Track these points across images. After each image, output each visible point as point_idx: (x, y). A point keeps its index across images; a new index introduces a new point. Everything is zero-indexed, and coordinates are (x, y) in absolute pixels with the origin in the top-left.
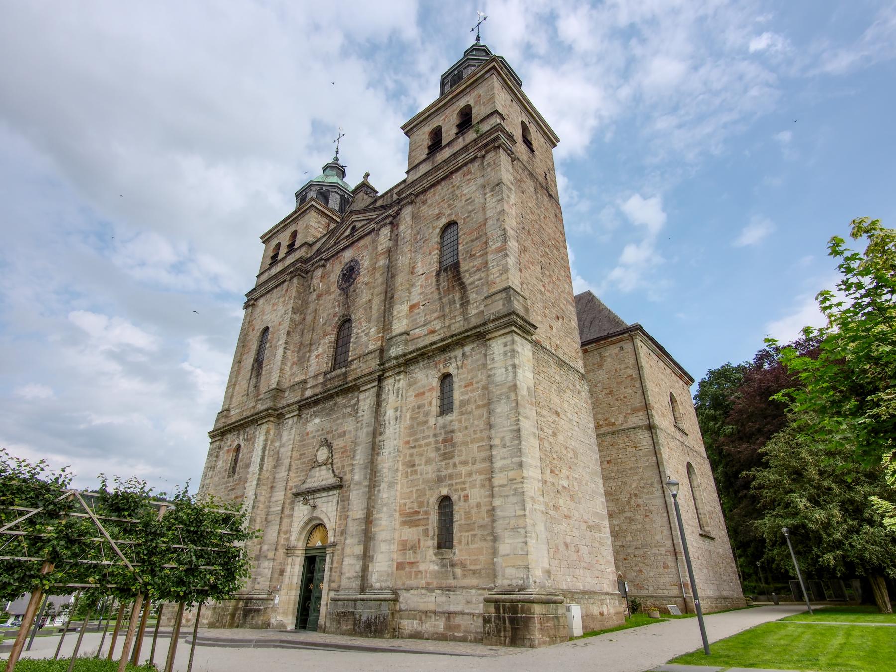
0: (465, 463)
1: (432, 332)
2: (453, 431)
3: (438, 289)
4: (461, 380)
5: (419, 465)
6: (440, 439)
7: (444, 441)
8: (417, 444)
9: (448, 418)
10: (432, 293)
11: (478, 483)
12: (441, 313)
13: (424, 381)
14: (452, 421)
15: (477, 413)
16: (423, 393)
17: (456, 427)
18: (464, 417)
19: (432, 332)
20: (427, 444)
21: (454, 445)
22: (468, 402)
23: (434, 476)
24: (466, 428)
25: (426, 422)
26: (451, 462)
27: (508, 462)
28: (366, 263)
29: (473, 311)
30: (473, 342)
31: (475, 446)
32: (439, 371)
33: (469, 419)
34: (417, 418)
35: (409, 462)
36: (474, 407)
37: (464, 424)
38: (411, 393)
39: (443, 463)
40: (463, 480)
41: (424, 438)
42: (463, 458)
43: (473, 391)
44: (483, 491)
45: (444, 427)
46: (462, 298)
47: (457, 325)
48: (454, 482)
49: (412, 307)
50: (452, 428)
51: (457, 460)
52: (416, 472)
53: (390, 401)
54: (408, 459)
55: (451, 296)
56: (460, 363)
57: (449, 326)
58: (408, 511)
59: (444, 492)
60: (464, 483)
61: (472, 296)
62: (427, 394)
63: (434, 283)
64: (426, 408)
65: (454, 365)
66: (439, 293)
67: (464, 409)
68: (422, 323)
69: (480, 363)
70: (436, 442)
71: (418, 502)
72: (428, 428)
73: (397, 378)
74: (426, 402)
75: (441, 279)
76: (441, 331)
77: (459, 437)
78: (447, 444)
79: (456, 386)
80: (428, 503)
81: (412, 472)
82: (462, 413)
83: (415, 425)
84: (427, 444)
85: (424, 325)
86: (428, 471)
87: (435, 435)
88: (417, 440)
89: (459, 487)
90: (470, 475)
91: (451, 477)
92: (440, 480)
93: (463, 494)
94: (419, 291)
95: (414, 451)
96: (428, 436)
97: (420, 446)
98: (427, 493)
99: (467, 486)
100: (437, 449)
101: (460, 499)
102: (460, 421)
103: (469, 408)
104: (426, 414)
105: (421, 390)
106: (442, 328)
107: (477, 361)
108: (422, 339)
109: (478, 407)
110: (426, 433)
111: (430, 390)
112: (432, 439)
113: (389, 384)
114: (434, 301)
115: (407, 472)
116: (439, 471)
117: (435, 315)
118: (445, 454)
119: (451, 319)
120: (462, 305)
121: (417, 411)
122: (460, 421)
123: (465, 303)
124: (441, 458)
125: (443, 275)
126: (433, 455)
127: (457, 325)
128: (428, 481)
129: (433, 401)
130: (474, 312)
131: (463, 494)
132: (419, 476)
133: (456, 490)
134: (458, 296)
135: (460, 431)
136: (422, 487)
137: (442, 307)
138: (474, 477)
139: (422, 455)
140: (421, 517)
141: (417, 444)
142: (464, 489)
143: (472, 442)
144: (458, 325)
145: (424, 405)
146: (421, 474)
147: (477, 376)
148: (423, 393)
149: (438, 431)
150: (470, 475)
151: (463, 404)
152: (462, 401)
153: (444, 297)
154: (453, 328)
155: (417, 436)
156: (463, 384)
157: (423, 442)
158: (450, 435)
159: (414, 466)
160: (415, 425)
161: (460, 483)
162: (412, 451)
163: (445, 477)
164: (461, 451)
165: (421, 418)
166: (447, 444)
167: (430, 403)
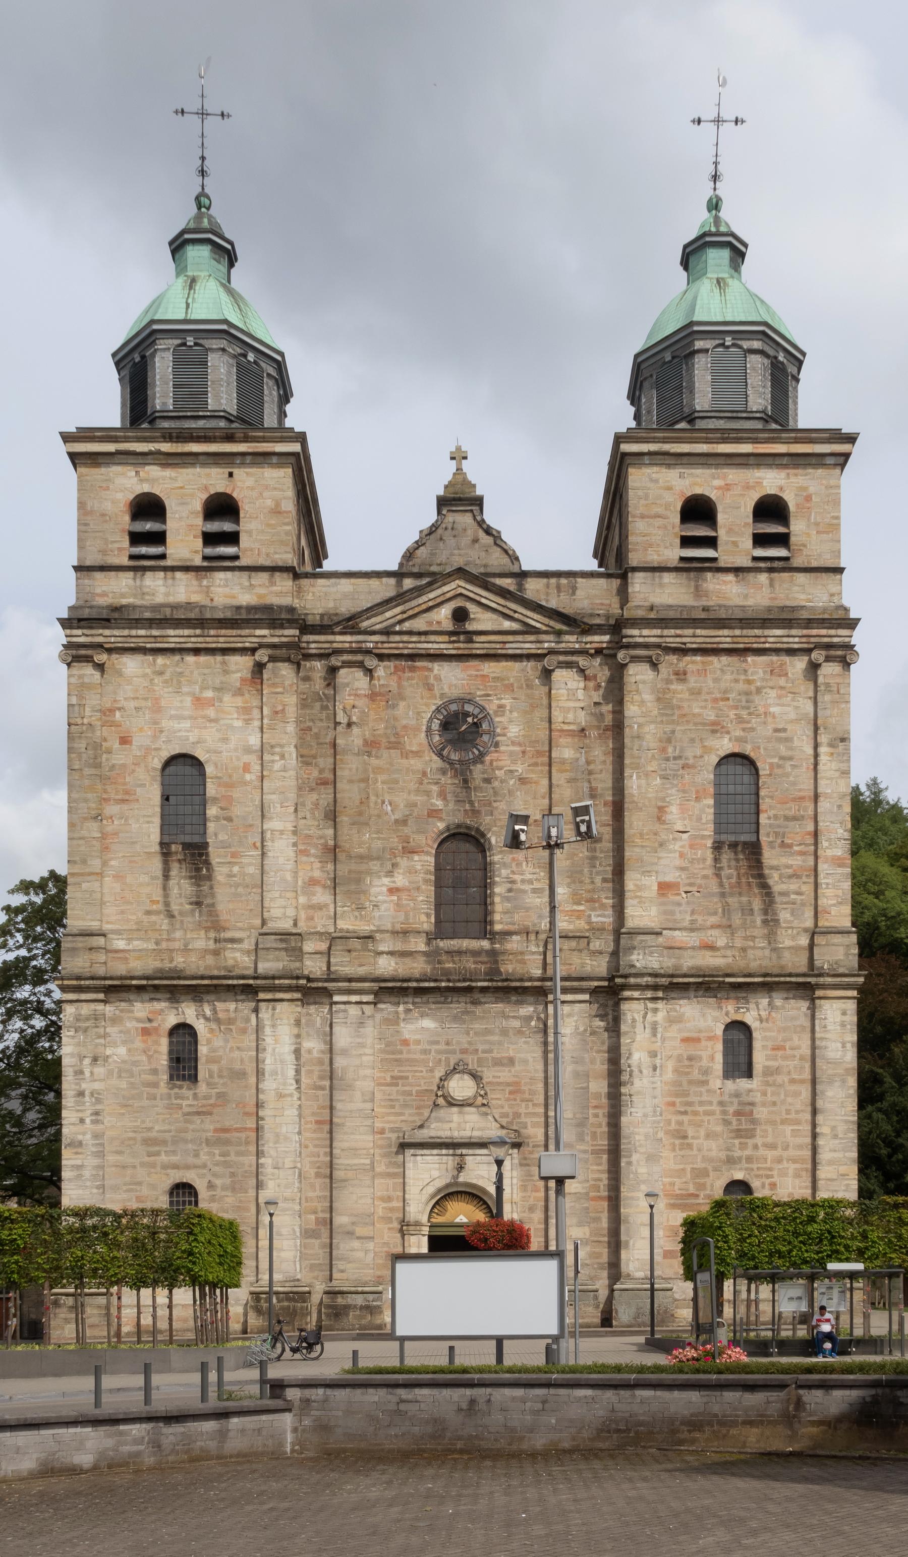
0: (772, 1147)
1: (711, 948)
2: (752, 1104)
3: (718, 876)
4: (765, 1038)
5: (693, 1138)
6: (731, 1110)
7: (738, 1113)
8: (689, 1109)
9: (743, 1084)
10: (705, 877)
11: (791, 1172)
12: (725, 922)
13: (702, 1024)
14: (750, 1091)
15: (793, 1088)
16: (698, 1040)
17: (758, 1098)
18: (770, 1090)
19: (711, 948)
20: (707, 1113)
21: (754, 1122)
22: (778, 1071)
23: (723, 1155)
24: (774, 1104)
25: (705, 1083)
26: (750, 1142)
27: (839, 1155)
28: (512, 726)
29: (786, 940)
30: (788, 990)
31: (788, 1129)
32: (727, 1014)
33: (779, 1094)
34: (688, 1073)
35: (678, 1131)
36: (786, 1080)
37: (769, 1098)
38: (674, 1032)
39: (737, 1141)
40: (768, 1165)
41: (701, 1103)
42: (770, 1140)
43: (785, 1058)
44: (797, 1181)
45: (737, 1095)
46: (765, 912)
47: (759, 953)
48: (755, 1166)
49: (664, 888)
50: (750, 1099)
51: (759, 1141)
52: (690, 1146)
53: (638, 1038)
54: (673, 1126)
55: (744, 899)
56: (764, 1014)
57: (744, 950)
58: (678, 1192)
59: (739, 1176)
60: (770, 1169)
61: (784, 915)
62: (704, 1043)
63: (709, 861)
64: (705, 1063)
65: (754, 1013)
66: (721, 885)
67: (770, 1079)
68: (686, 924)
69: (798, 1023)
70: (724, 1112)
71: (695, 1184)
72: (708, 1091)
73: (650, 1005)
74: (704, 1055)
75: (724, 863)
76: (729, 953)
77: (761, 1113)
78: (743, 1121)
79: (757, 1045)
80: (712, 1186)
81: (682, 1144)
82: (767, 1084)
83: (685, 1083)
84: (707, 1113)
85: (692, 930)
86: (714, 1149)
87: (721, 1103)
88: (690, 1104)
89: (761, 1172)
90: (779, 1160)
91: (749, 1159)
92: (731, 1161)
93: (768, 1181)
94: (678, 862)
95: (685, 1118)
96: (711, 1103)
97: (695, 1113)
98: (711, 1174)
99: (775, 1173)
100: (727, 1123)
101: (763, 1186)
102: (764, 1094)
103: (779, 1079)
104: (706, 1072)
105: (695, 1035)
106: (727, 947)
107: (793, 1018)
108: (690, 952)
109: (793, 1081)
110: (705, 1098)
111: (710, 1038)
112: (715, 1108)
113: (633, 1010)
114: (712, 895)
115: (674, 1144)
116: (728, 1149)
117: (713, 920)
118: (738, 1130)
119: (746, 938)
120: (765, 922)
121: (686, 1063)
122: (764, 1094)
123: (771, 922)
124: (732, 1135)
125: (727, 856)
126: (719, 1129)
127: (759, 953)
128: (711, 1160)
129: (714, 1055)
130: (788, 943)
131: (768, 1181)
132: (695, 1152)
133: (757, 1176)
134: (757, 904)
135: (764, 1104)
136: (700, 1165)
137: (727, 911)
138: (785, 1164)
139: (700, 1126)
140: (701, 1201)
141: (689, 1109)
142: (772, 1176)
143: (783, 1122)
144: (759, 958)
145: (700, 1058)
146: (699, 1150)
147: (791, 1039)
148: (698, 1040)
149: (726, 1098)
150: (779, 1160)
151: (768, 1072)
152: (765, 1067)
153: (732, 895)
154: (750, 953)
155: (689, 1099)
156: (770, 1044)
157: (701, 1109)
158: (748, 1108)
159: (685, 1137)
160: (685, 1083)
161: (765, 1169)
162: (680, 1118)
163: (740, 1158)
164: (766, 1131)
165: (696, 1075)
166: (743, 1121)
167: (712, 1058)
